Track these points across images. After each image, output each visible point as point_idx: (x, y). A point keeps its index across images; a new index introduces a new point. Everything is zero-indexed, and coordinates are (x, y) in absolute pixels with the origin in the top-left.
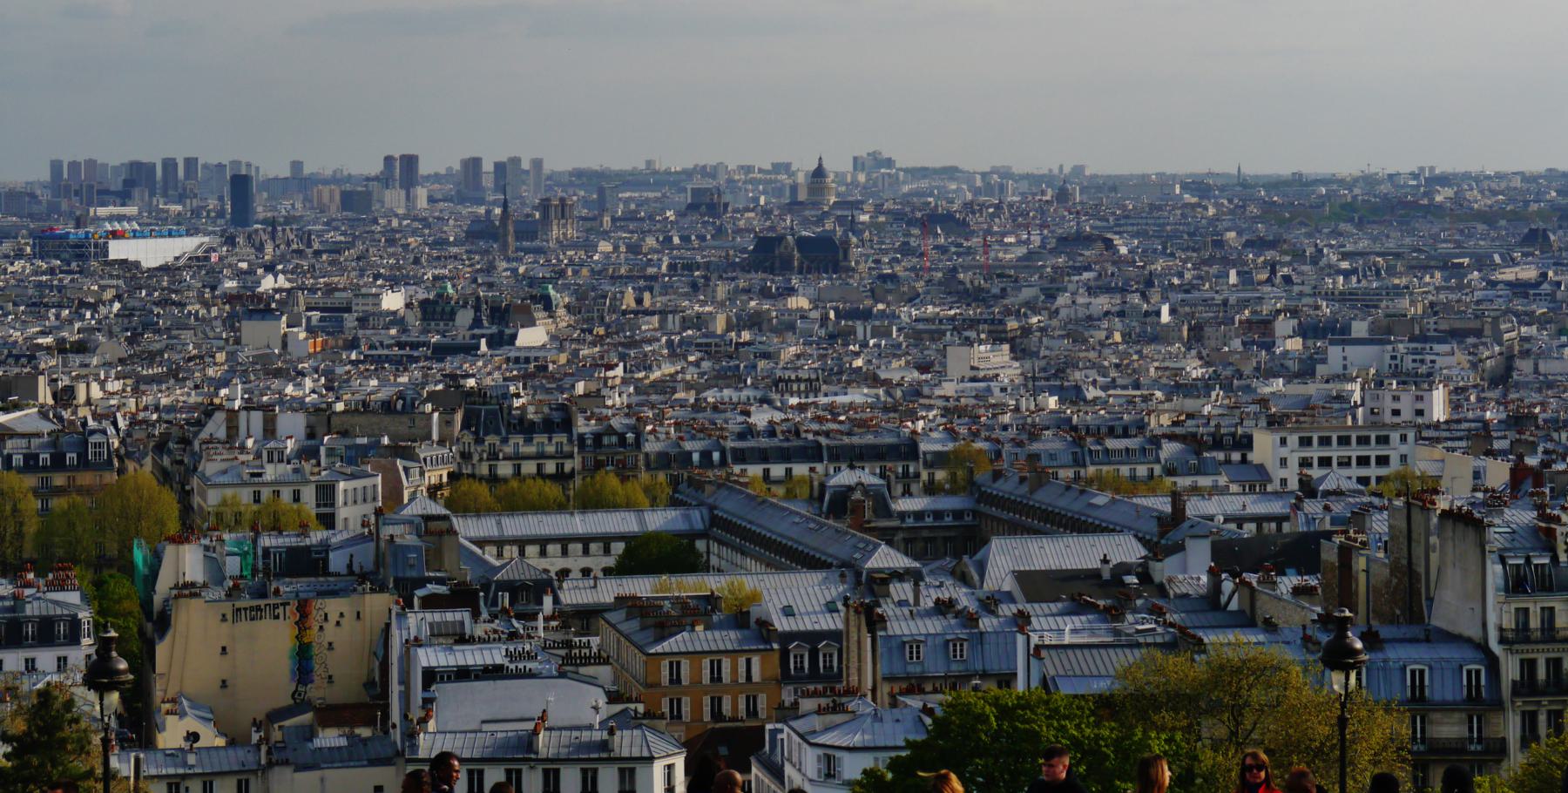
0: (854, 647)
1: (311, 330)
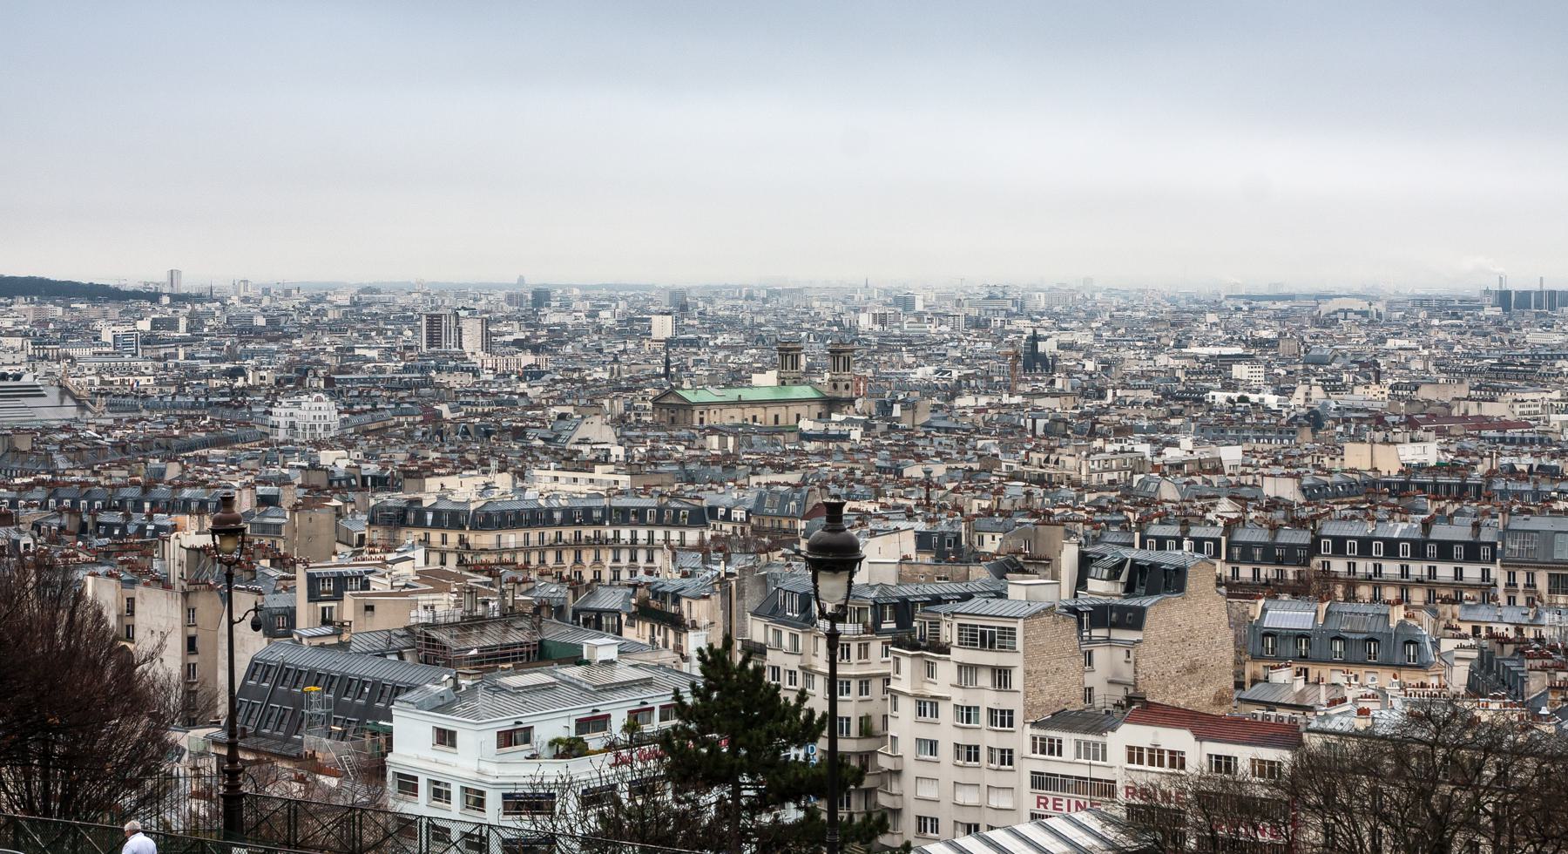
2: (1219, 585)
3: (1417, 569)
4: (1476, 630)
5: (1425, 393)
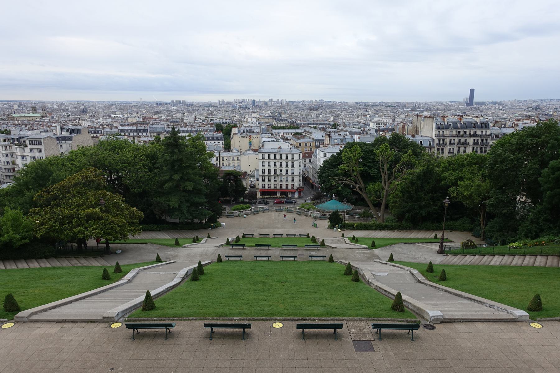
0: (326, 141)
1: (260, 115)
2: (89, 132)
3: (136, 134)
4: (144, 141)
5: (145, 115)
